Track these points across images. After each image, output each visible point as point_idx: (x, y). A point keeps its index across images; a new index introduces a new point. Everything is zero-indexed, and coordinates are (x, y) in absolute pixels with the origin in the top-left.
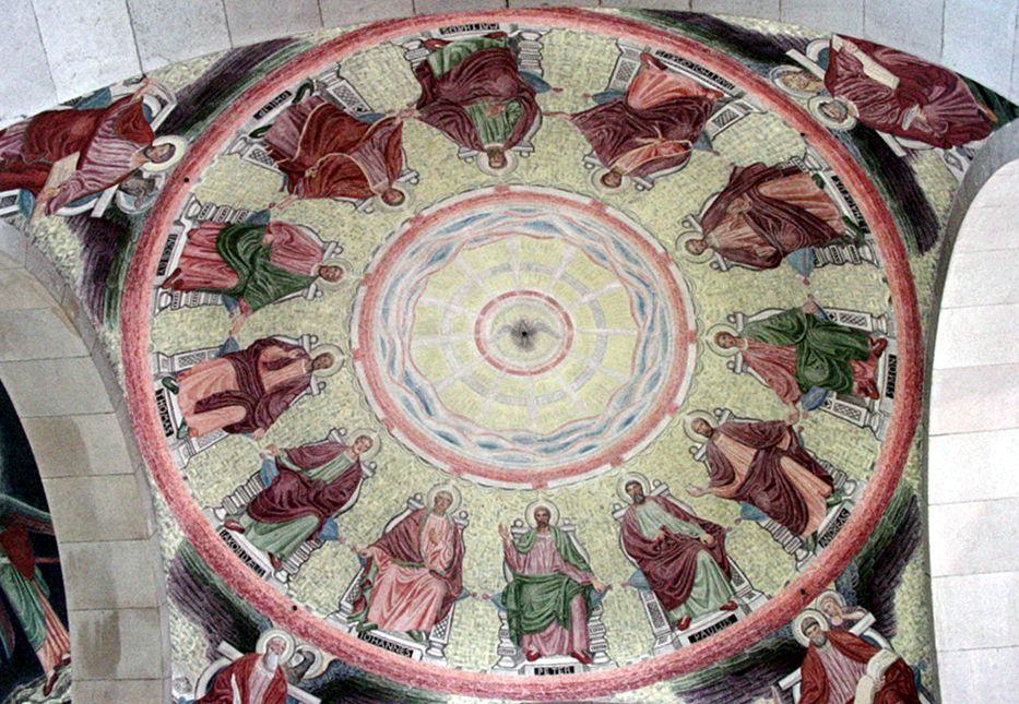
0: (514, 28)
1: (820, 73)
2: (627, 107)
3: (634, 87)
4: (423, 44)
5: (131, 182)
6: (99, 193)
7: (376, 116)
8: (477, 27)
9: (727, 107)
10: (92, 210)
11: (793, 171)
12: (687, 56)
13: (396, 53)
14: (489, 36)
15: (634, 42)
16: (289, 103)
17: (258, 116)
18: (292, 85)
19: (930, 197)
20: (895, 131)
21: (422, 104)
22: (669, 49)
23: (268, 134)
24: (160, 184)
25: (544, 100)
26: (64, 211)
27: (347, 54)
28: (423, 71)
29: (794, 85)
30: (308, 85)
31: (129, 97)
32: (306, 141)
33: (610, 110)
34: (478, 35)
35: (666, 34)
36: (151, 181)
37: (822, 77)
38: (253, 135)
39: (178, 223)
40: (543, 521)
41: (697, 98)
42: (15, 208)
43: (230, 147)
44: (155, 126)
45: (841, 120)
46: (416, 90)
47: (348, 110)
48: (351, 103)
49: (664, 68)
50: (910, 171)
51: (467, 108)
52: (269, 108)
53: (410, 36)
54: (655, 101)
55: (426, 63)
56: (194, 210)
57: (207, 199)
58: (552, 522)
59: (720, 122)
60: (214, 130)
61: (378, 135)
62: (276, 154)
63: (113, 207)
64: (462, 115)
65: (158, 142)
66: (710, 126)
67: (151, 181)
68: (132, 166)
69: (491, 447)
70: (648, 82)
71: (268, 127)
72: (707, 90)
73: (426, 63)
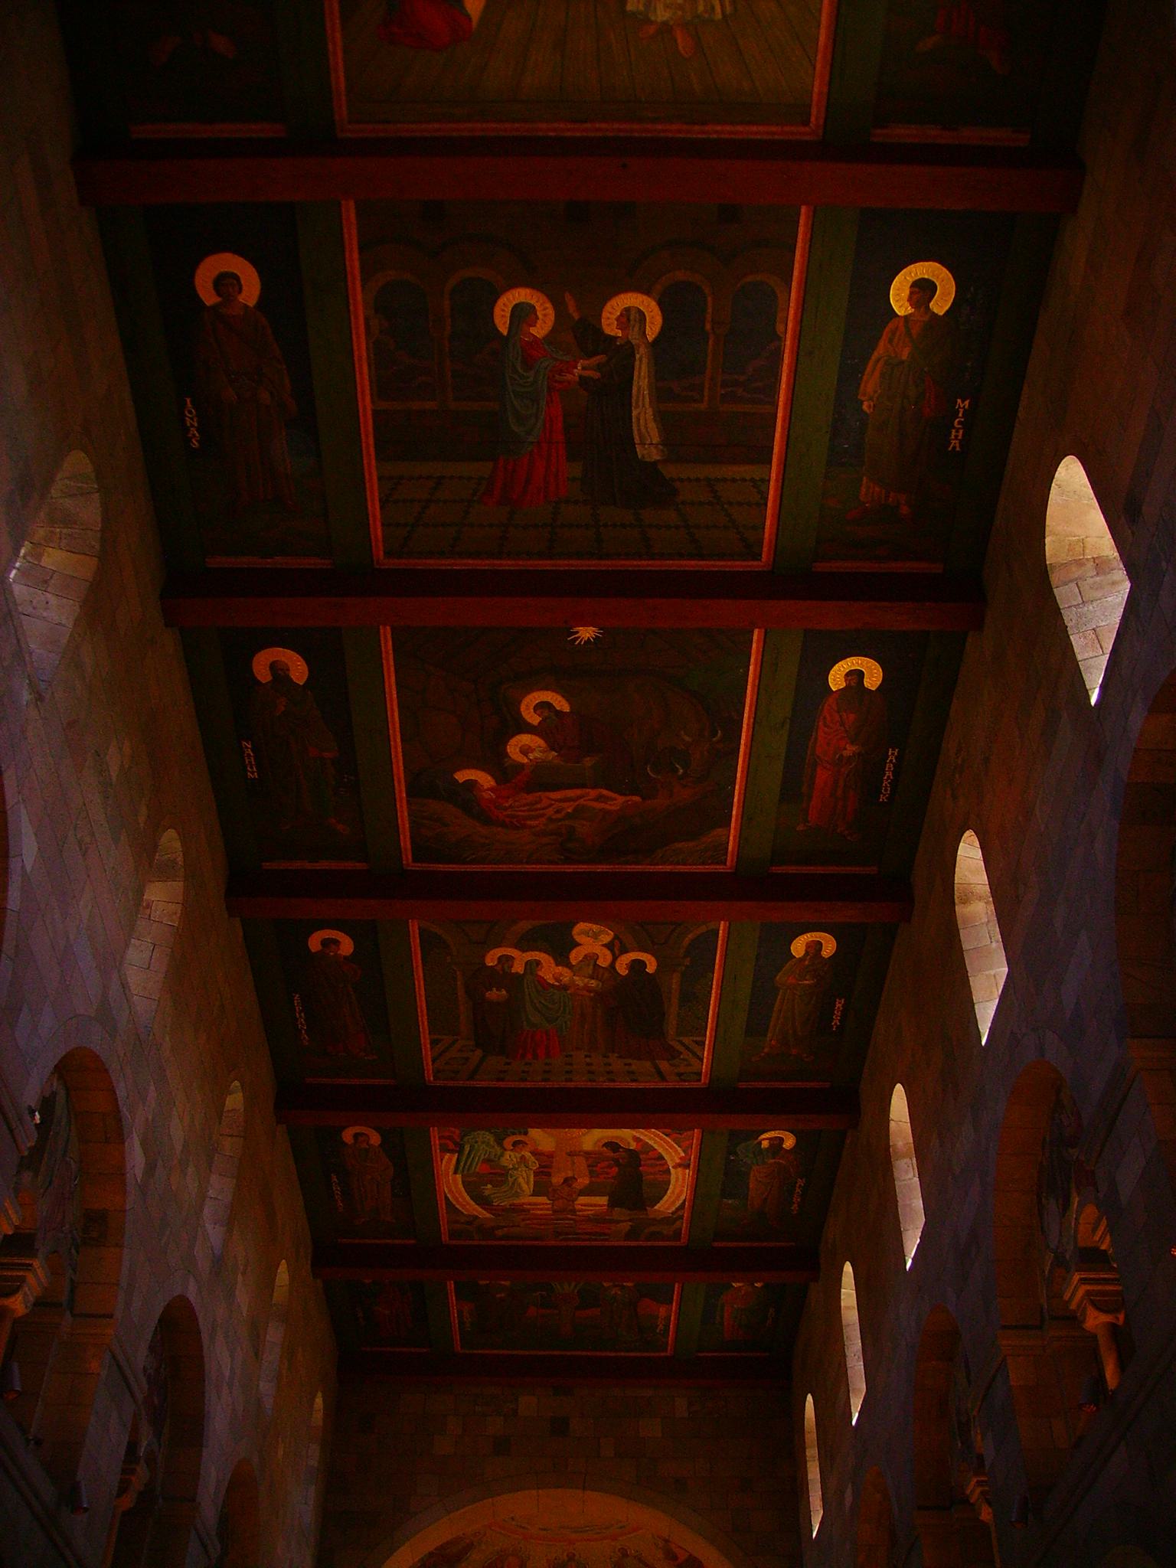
40: (571, 1557)
58: (576, 1558)
69: (545, 1530)
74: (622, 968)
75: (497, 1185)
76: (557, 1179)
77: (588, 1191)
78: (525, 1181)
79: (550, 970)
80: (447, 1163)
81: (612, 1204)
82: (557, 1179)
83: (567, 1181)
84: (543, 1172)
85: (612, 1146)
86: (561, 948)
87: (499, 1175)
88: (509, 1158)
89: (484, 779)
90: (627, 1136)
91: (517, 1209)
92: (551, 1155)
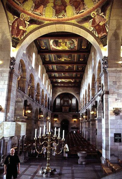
0: (55, 18)
1: (26, 22)
2: (43, 5)
3: (43, 9)
4: (65, 16)
5: (98, 14)
6: (101, 16)
7: (71, 5)
8: (59, 18)
9: (33, 9)
10: (103, 14)
11: (23, 3)
12: (38, 16)
13: (68, 15)
14: (58, 16)
15: (44, 17)
16: (80, 12)
17: (83, 12)
18: (79, 15)
19: (10, 13)
20: (17, 20)
21: (66, 6)
22: (40, 17)
23: (83, 8)
24: (96, 10)
25: (52, 5)
26: (105, 18)
27: (72, 17)
28: (65, 12)
29: (27, 17)
30: (77, 14)
31: (92, 27)
32: (80, 4)
33: (45, 4)
34: (59, 16)
35: (41, 19)
36: (96, 12)
37: (25, 22)
38: (85, 9)
39: (97, 2)
41: (36, 9)
42: (107, 25)
43: (87, 9)
44: (92, 20)
45: (22, 15)
46: (67, 8)
47: (74, 7)
48: (74, 9)
49: (40, 13)
50: (13, 15)
51: (61, 4)
52: (82, 12)
53: (66, 18)
54: (41, 7)
55: (65, 13)
56: (95, 3)
57: (93, 3)
59: (33, 6)
60: (88, 13)
61: (72, 2)
62: (84, 4)
63: (101, 12)
64: (62, 3)
65: (93, 17)
66: (34, 5)
67: (96, 12)
68: (97, 16)
70: (42, 10)
71: (83, 9)
72: (35, 11)
73: (65, 13)
74: (60, 59)
75: (71, 43)
76: (64, 43)
77: (61, 42)
78: (68, 43)
79: (66, 59)
80: (76, 45)
81: (58, 41)
82: (64, 43)
83: (63, 43)
84: (66, 44)
85: (59, 47)
86: (65, 60)
87: (71, 44)
88: (69, 46)
89: (70, 66)
90: (58, 48)
91: (69, 40)
92: (65, 46)
